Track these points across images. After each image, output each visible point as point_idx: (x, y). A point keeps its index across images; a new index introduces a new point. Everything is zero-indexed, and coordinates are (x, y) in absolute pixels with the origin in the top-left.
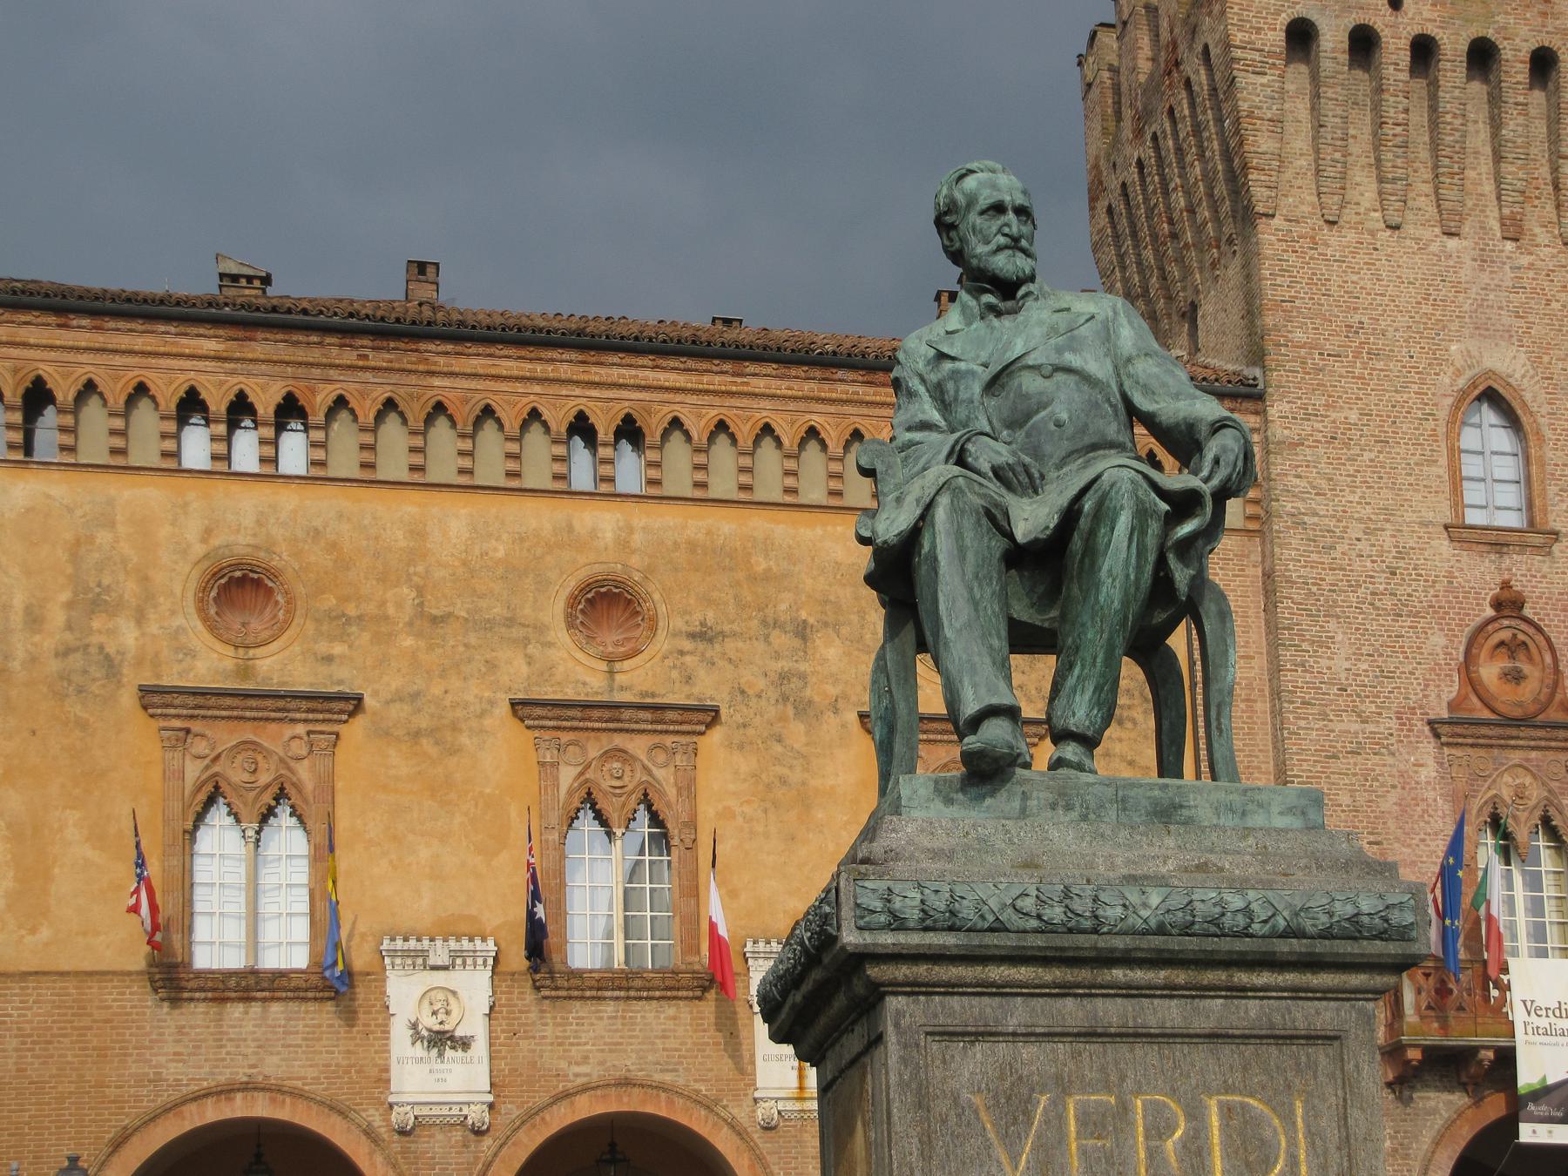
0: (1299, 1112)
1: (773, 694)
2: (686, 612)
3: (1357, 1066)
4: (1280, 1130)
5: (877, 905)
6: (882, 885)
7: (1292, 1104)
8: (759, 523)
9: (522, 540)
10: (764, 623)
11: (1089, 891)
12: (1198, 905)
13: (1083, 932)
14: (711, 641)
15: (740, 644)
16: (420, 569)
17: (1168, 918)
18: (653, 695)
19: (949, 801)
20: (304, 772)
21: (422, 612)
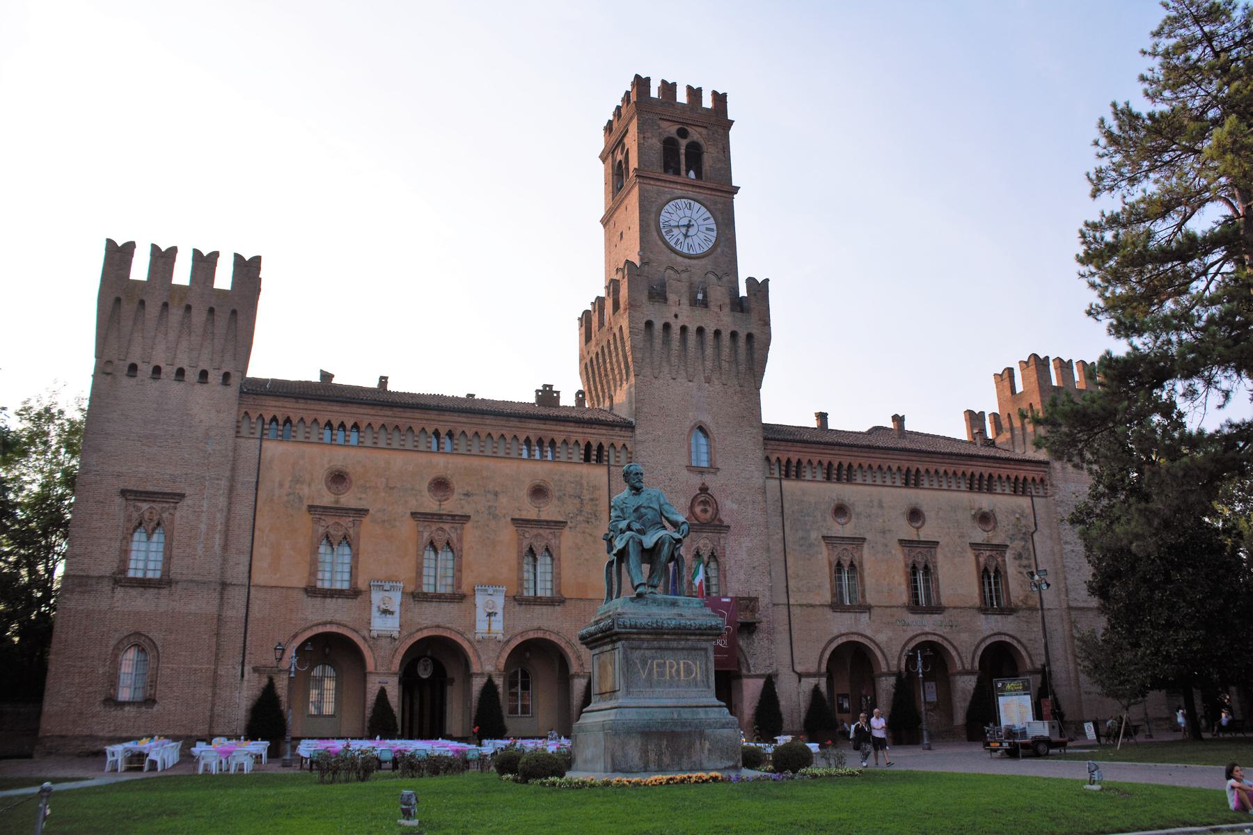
8: (486, 462)
20: (351, 532)
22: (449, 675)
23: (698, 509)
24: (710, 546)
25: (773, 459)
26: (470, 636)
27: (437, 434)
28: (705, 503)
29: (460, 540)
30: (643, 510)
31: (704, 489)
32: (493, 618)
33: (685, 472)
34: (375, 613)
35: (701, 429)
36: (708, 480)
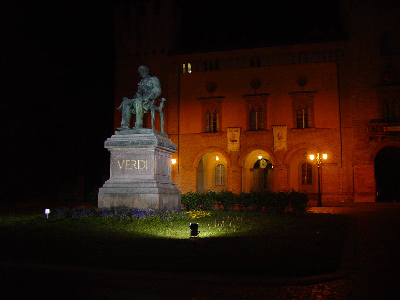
0: (147, 161)
32: (282, 140)
34: (229, 142)
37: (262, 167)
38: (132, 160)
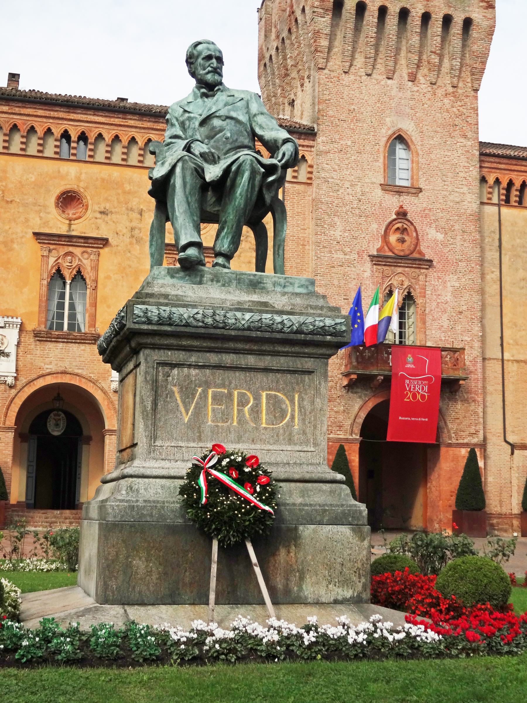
0: (296, 399)
1: (129, 235)
2: (99, 204)
3: (320, 383)
4: (289, 405)
5: (142, 314)
6: (143, 307)
7: (294, 396)
9: (41, 175)
10: (127, 209)
11: (223, 312)
12: (264, 320)
13: (220, 328)
14: (107, 214)
15: (118, 216)
16: (4, 184)
17: (252, 324)
18: (85, 233)
19: (172, 277)
21: (3, 200)
22: (85, 432)
23: (393, 238)
24: (406, 284)
25: (491, 180)
26: (104, 385)
27: (66, 135)
28: (404, 231)
29: (96, 268)
30: (216, 122)
31: (402, 214)
33: (379, 192)
35: (400, 139)
36: (409, 202)
37: (53, 431)
38: (236, 388)
